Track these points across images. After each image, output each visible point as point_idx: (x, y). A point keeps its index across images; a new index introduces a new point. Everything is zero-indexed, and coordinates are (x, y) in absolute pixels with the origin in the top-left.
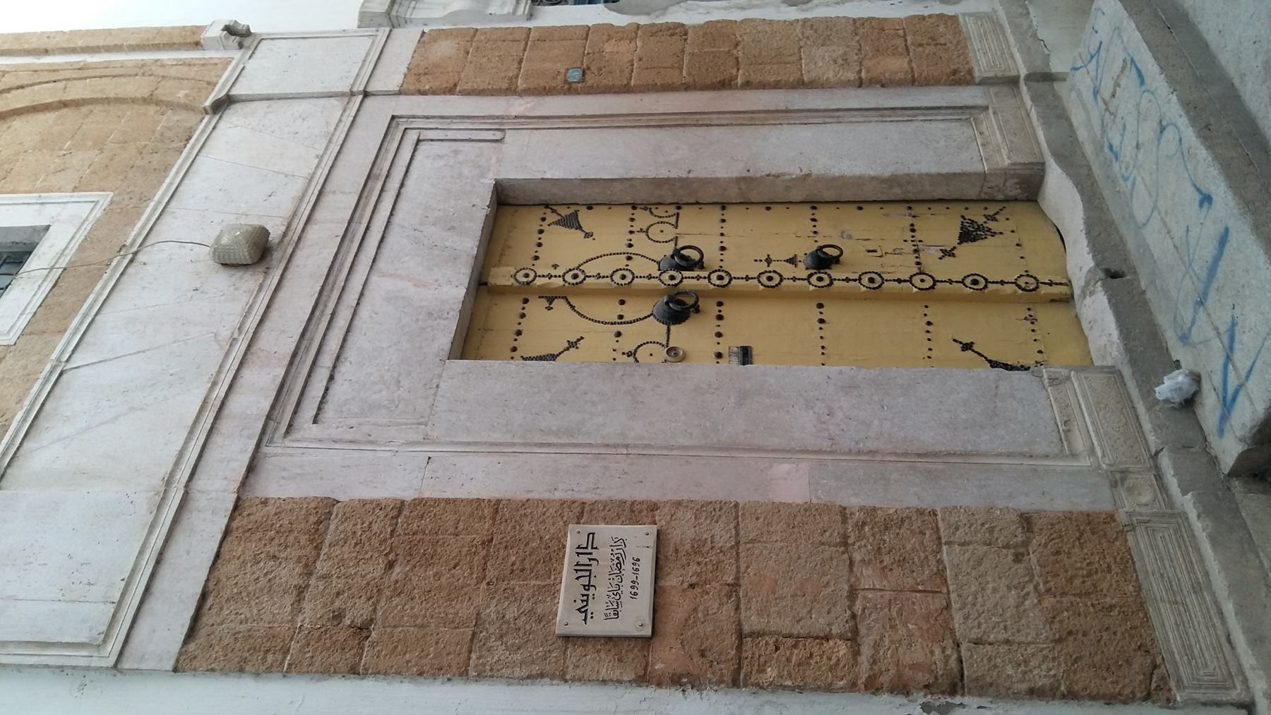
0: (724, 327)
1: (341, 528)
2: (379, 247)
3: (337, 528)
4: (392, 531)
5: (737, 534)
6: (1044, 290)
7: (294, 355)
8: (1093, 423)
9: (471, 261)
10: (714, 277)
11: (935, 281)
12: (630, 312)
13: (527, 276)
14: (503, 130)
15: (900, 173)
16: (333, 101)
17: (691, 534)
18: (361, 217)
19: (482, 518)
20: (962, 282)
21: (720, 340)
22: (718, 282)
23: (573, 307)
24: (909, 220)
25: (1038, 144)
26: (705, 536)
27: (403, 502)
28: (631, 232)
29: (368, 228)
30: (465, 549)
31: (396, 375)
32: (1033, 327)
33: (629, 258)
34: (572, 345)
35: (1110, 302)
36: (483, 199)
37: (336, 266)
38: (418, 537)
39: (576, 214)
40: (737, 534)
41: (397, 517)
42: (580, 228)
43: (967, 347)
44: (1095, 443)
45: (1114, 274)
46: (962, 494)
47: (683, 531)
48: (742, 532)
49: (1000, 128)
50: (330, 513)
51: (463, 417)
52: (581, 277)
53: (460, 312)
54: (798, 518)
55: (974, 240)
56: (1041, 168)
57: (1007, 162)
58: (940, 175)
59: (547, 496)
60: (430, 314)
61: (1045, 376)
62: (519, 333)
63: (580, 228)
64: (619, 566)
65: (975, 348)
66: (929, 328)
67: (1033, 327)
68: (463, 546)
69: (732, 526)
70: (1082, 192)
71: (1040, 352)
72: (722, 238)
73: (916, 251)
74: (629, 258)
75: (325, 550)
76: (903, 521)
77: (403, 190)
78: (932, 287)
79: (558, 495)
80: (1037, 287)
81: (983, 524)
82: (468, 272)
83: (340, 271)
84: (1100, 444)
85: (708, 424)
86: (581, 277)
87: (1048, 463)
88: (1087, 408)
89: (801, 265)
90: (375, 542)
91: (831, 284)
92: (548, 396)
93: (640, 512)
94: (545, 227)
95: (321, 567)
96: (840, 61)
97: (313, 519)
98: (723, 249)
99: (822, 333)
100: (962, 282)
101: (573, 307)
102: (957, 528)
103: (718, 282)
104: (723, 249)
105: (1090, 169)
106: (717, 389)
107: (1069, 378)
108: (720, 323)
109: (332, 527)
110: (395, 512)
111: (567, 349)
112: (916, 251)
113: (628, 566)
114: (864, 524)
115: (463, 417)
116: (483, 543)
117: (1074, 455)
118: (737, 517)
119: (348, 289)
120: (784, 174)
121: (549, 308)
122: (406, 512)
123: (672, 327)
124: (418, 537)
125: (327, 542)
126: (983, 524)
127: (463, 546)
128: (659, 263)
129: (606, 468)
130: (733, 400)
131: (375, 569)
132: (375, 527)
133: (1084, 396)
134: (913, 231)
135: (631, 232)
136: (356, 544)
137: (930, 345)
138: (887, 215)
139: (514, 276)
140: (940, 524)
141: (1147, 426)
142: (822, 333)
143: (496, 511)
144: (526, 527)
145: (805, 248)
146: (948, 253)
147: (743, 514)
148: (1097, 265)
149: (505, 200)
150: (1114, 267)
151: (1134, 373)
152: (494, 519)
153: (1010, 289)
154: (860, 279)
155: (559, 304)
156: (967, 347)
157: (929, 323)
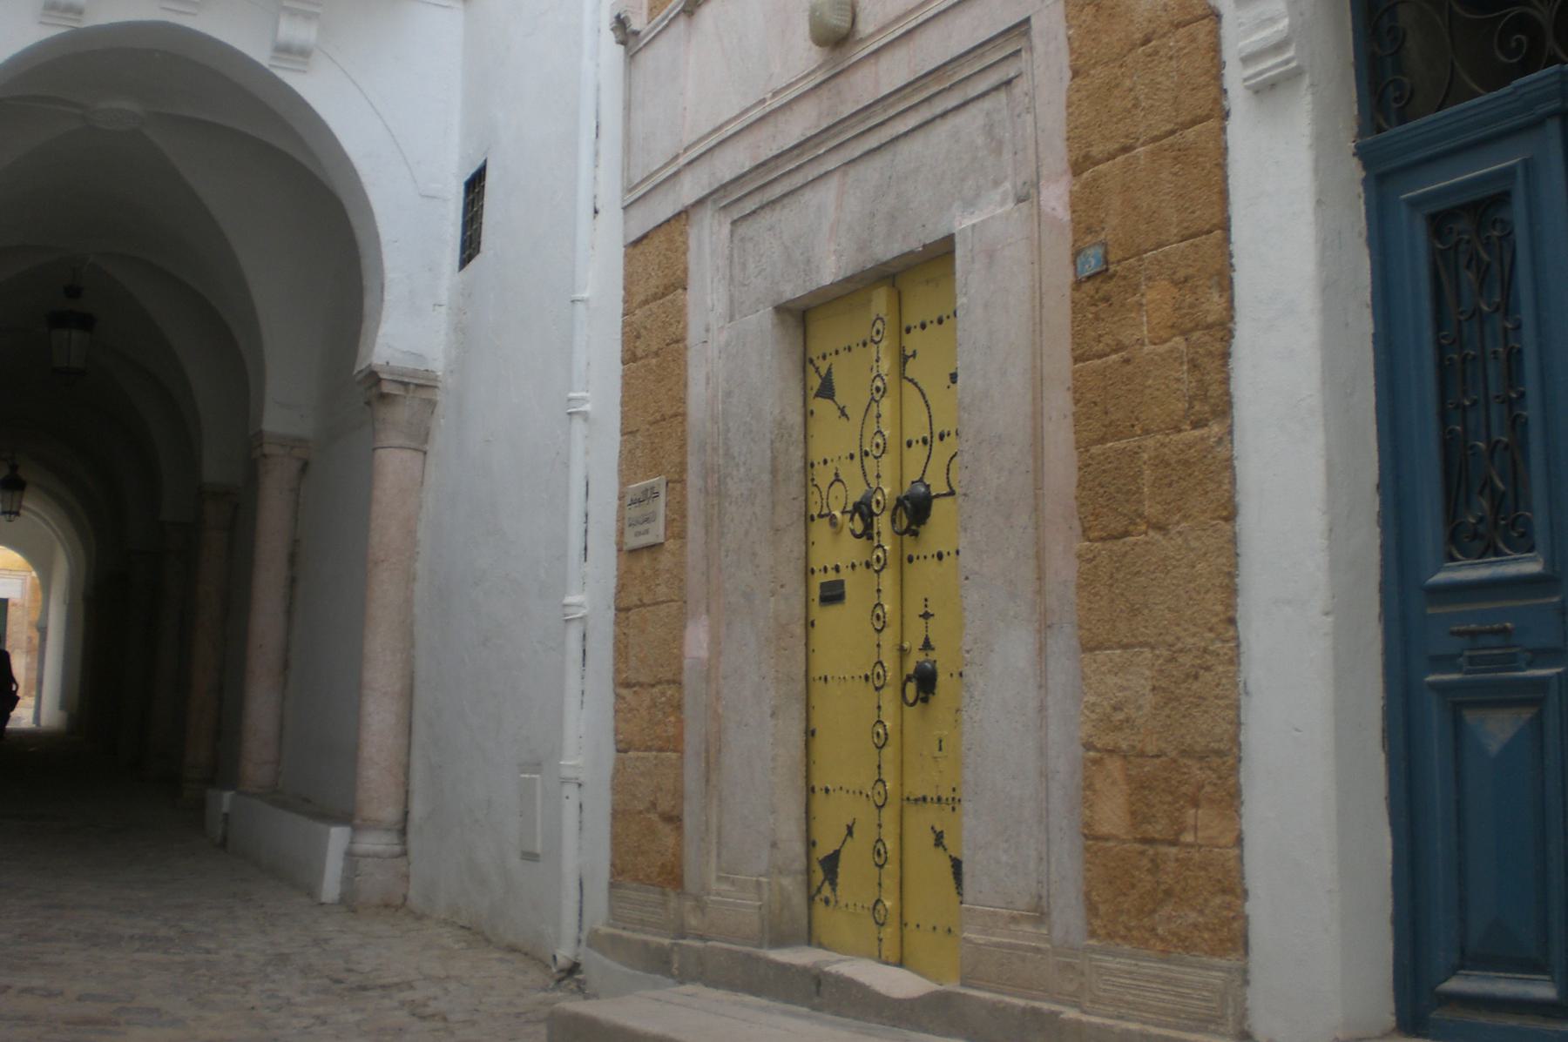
0: (861, 569)
2: (861, 157)
7: (763, 164)
16: (849, 19)
18: (892, 105)
29: (882, 124)
33: (867, 454)
37: (836, 130)
47: (666, 560)
49: (1010, 946)
60: (808, 261)
64: (647, 520)
73: (939, 799)
74: (925, 441)
77: (938, 121)
83: (835, 136)
89: (921, 657)
95: (653, 306)
96: (1120, 716)
98: (940, 556)
104: (940, 556)
112: (939, 799)
113: (646, 526)
117: (719, 879)
119: (892, 123)
128: (921, 480)
131: (654, 348)
146: (939, 839)
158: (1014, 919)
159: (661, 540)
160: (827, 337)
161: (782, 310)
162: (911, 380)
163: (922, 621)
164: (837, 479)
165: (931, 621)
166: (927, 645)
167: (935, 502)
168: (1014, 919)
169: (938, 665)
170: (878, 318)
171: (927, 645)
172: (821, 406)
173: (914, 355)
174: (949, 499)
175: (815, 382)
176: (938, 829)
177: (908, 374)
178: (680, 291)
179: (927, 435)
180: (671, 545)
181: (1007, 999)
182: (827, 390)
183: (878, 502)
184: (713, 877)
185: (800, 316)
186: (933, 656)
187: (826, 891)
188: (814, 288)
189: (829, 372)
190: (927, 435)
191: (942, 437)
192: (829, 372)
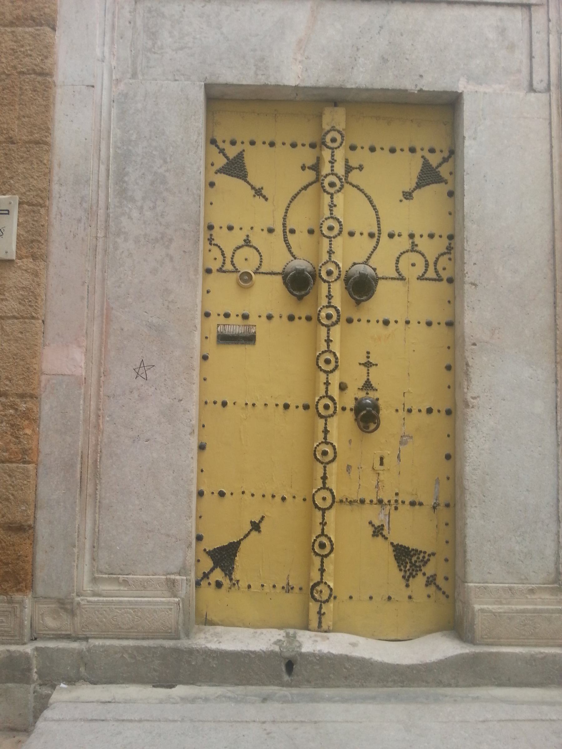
1: (27, 36)
3: (26, 33)
4: (23, 73)
5: (9, 318)
6: (314, 607)
8: (121, 602)
9: (336, 85)
10: (331, 311)
11: (324, 510)
12: (299, 241)
13: (334, 140)
14: (548, 89)
15: (468, 497)
17: (9, 283)
19: (32, 133)
20: (323, 534)
21: (264, 318)
22: (323, 314)
23: (305, 188)
24: (429, 501)
25: (501, 645)
26: (7, 294)
27: (50, 74)
28: (412, 236)
30: (5, 126)
31: (190, 45)
32: (279, 586)
34: (258, 192)
35: (254, 652)
36: (433, 81)
38: (18, 92)
39: (439, 180)
40: (9, 318)
41: (35, 72)
42: (419, 186)
43: (256, 526)
44: (101, 599)
45: (289, 668)
46: (51, 488)
48: (10, 321)
49: (535, 611)
50: (41, 25)
51: (139, 106)
52: (332, 190)
53: (266, 85)
54: (22, 363)
55: (398, 558)
56: (472, 641)
57: (477, 607)
58: (465, 536)
59: (55, 178)
60: (262, 59)
61: (178, 577)
62: (272, 144)
63: (419, 186)
65: (254, 533)
66: (278, 499)
67: (279, 586)
68: (8, 124)
69: (16, 314)
70: (411, 668)
71: (249, 587)
72: (402, 323)
75: (9, 29)
76: (17, 438)
78: (316, 506)
79: (55, 188)
80: (316, 600)
81: (13, 495)
82: (321, 84)
84: (98, 602)
85: (130, 300)
86: (332, 190)
87: (87, 557)
88: (136, 602)
89: (361, 395)
90: (15, 62)
91: (321, 416)
92: (161, 171)
93: (32, 248)
94: (419, 153)
97: (35, 14)
99: (271, 406)
100: (323, 534)
101: (305, 188)
102: (10, 476)
103: (323, 314)
104: (386, 323)
105: (444, 686)
106: (168, 308)
107: (175, 596)
108: (285, 318)
109: (27, 29)
110: (37, 69)
111: (253, 188)
114: (16, 410)
115: (139, 106)
116: (11, 138)
118: (23, 317)
120: (469, 380)
121: (303, 168)
122: (39, 78)
123: (279, 278)
124: (18, 92)
125: (13, 29)
126: (13, 495)
127: (8, 124)
128: (366, 263)
129: (79, 221)
130: (155, 320)
132: (27, 59)
133: (149, 602)
134: (413, 504)
135: (412, 236)
136: (13, 49)
137: (258, 496)
138: (437, 481)
139: (333, 129)
140: (14, 465)
141: (108, 642)
142: (271, 406)
143: (37, 143)
144: (21, 166)
145: (387, 397)
146: (378, 531)
147: (25, 323)
148: (301, 655)
149: (447, 106)
150: (296, 668)
151: (164, 648)
152: (30, 142)
153: (316, 576)
154: (327, 443)
155: (310, 175)
156: (256, 526)
157: (284, 499)
158: (532, 591)
159: (13, 256)
160: (236, 128)
161: (208, 87)
162: (357, 187)
163: (365, 369)
164: (247, 243)
165: (372, 369)
166: (368, 386)
167: (381, 282)
168: (532, 591)
169: (380, 402)
170: (333, 129)
171: (368, 386)
172: (223, 180)
173: (361, 168)
174: (400, 283)
175: (221, 161)
176: (377, 523)
177: (350, 179)
178: (48, 29)
179: (375, 230)
180: (28, 263)
181: (542, 650)
182: (236, 168)
183: (329, 273)
184: (86, 578)
185: (220, 100)
186: (373, 395)
187: (218, 575)
188: (272, 81)
189: (240, 156)
190: (375, 230)
191: (391, 236)
192: (240, 156)
